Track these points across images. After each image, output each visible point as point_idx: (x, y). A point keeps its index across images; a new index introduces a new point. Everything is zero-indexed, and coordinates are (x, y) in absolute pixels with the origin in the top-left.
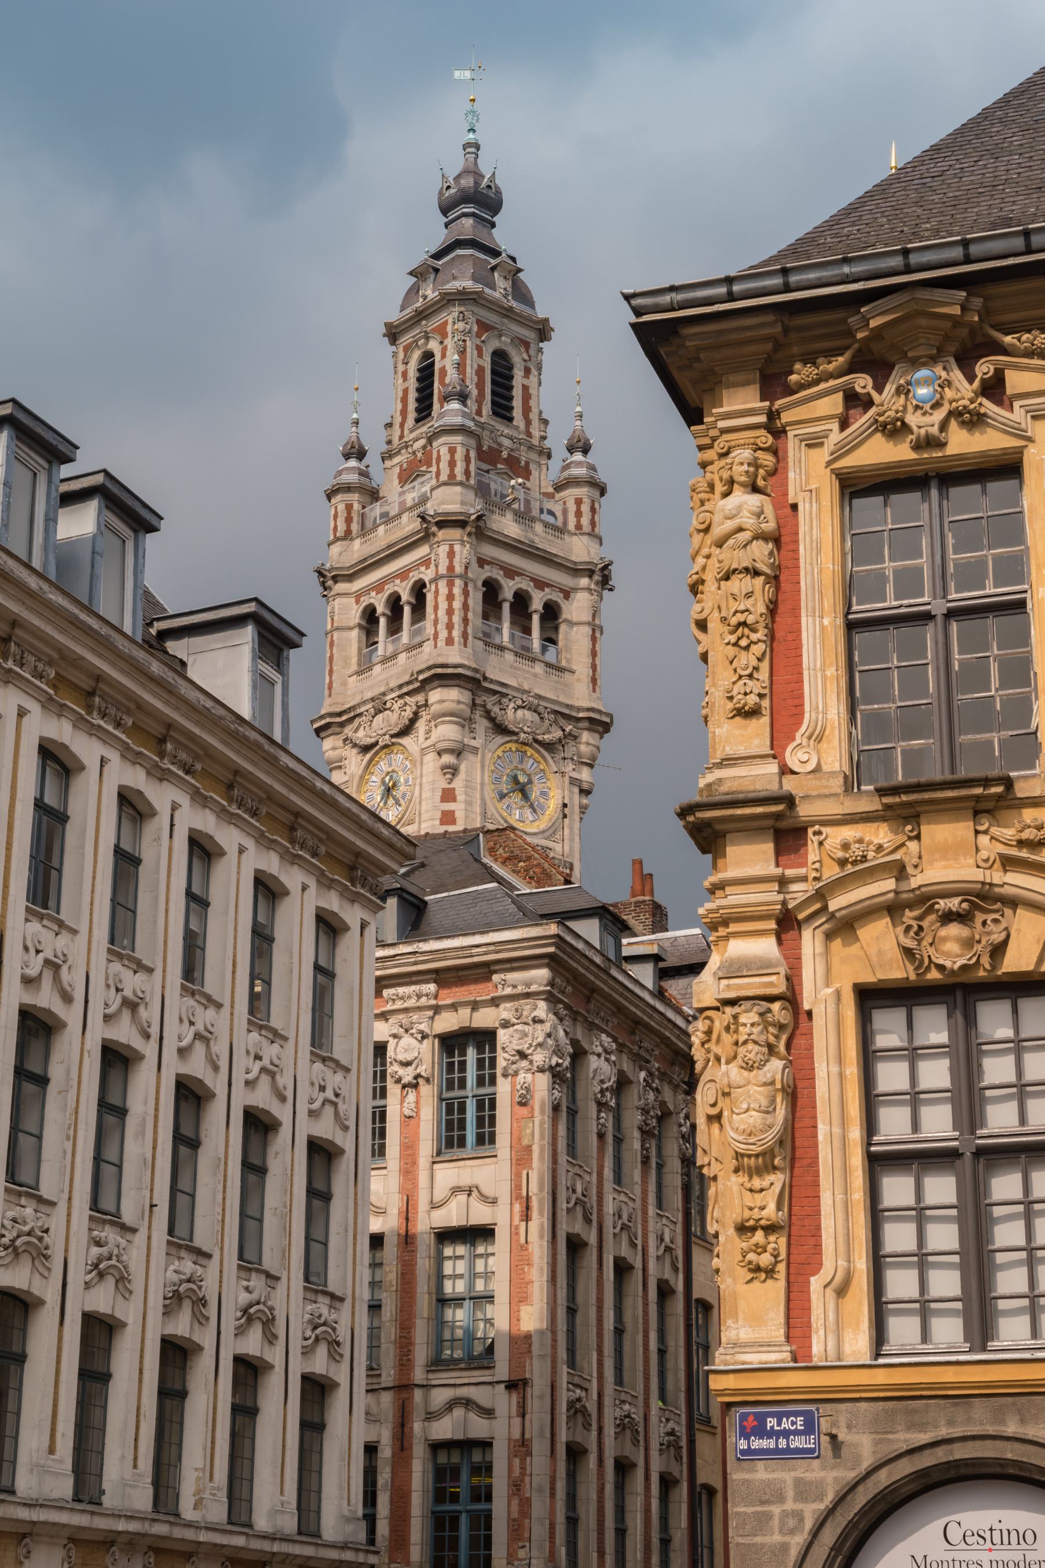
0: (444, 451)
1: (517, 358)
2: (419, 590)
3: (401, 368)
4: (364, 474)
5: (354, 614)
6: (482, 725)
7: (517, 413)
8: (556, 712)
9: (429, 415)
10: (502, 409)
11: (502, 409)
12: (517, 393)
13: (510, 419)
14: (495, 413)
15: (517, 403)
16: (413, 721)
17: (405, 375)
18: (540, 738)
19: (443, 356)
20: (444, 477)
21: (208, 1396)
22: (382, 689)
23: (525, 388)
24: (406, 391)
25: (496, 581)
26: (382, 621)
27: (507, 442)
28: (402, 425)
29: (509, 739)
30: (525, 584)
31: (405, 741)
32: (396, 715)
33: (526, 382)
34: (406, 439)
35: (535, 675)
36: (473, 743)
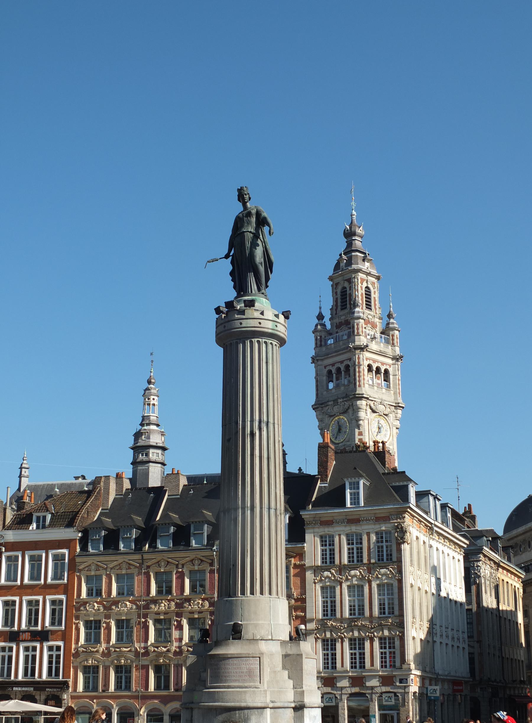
2: (347, 367)
3: (335, 291)
5: (325, 371)
6: (369, 411)
7: (373, 307)
9: (346, 308)
10: (369, 306)
11: (369, 306)
13: (371, 309)
14: (367, 308)
16: (347, 410)
17: (336, 293)
22: (336, 398)
23: (374, 298)
24: (337, 299)
26: (334, 375)
27: (370, 317)
28: (336, 310)
31: (345, 415)
32: (342, 407)
35: (383, 393)
36: (366, 417)
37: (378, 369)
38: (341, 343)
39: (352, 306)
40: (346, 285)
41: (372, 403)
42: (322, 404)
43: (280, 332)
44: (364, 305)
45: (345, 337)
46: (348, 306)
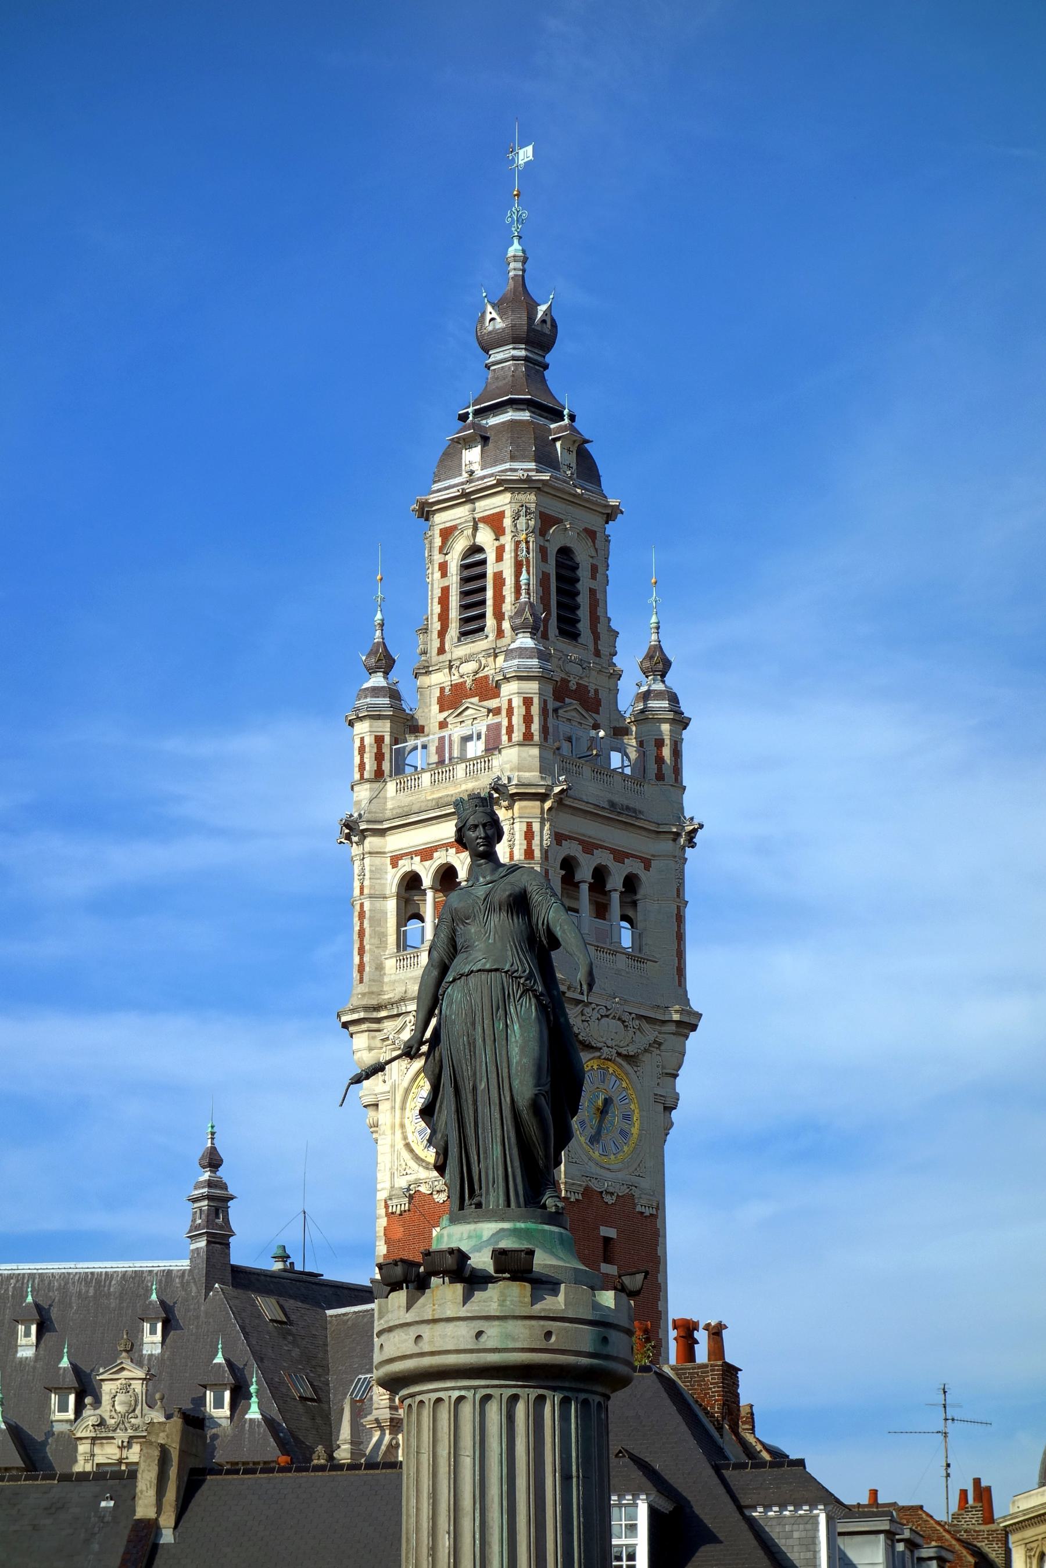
0: (517, 702)
1: (583, 556)
4: (394, 695)
5: (392, 879)
7: (584, 626)
8: (640, 1017)
9: (482, 629)
11: (569, 629)
12: (583, 600)
15: (583, 613)
18: (620, 1050)
19: (499, 558)
20: (517, 736)
23: (593, 592)
24: (445, 591)
25: (574, 858)
28: (442, 634)
29: (592, 1056)
30: (603, 858)
33: (593, 584)
34: (447, 657)
37: (600, 874)
38: (460, 770)
39: (506, 625)
40: (485, 537)
42: (377, 1008)
43: (615, 1359)
44: (553, 622)
45: (476, 748)
46: (490, 622)
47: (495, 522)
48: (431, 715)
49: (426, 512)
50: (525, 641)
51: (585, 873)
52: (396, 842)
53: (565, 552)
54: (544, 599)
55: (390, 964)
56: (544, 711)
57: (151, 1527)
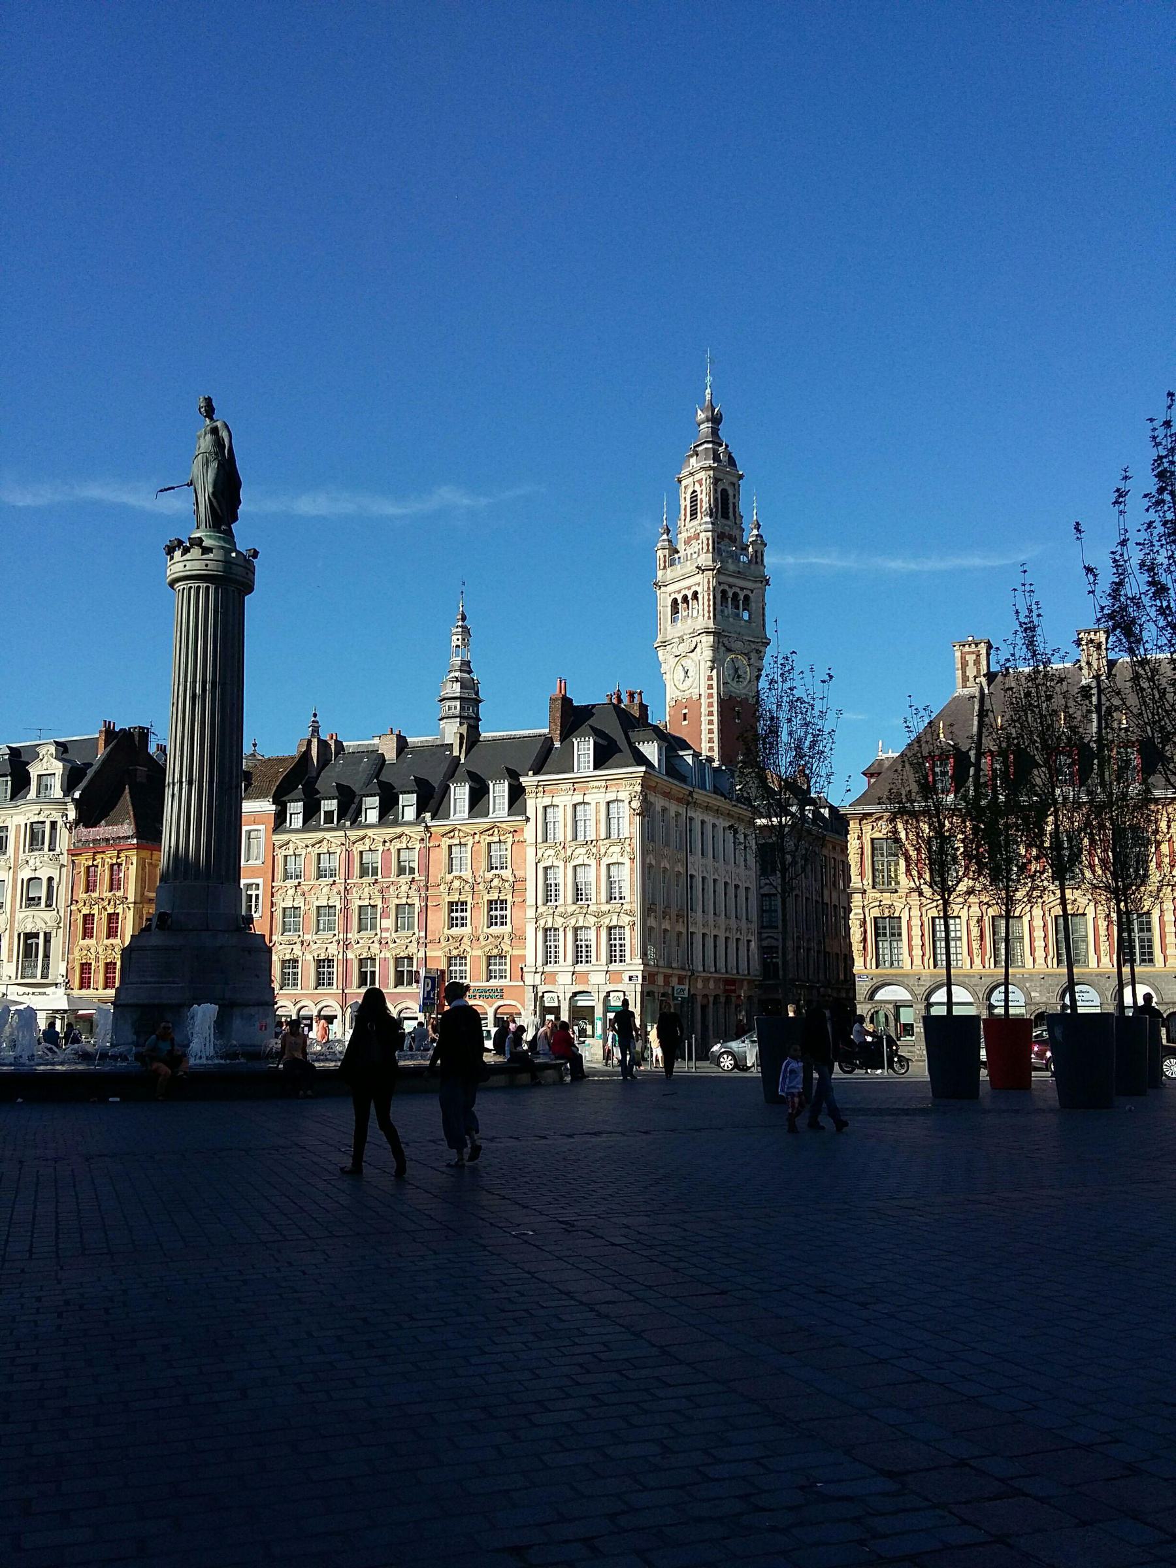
1: (731, 492)
2: (695, 594)
7: (731, 514)
11: (725, 515)
12: (731, 505)
15: (731, 510)
21: (732, 945)
37: (735, 595)
40: (697, 487)
41: (725, 640)
47: (700, 482)
48: (681, 547)
49: (680, 482)
50: (708, 519)
51: (730, 594)
52: (670, 588)
53: (724, 491)
54: (716, 506)
55: (669, 628)
56: (713, 542)
57: (458, 758)
